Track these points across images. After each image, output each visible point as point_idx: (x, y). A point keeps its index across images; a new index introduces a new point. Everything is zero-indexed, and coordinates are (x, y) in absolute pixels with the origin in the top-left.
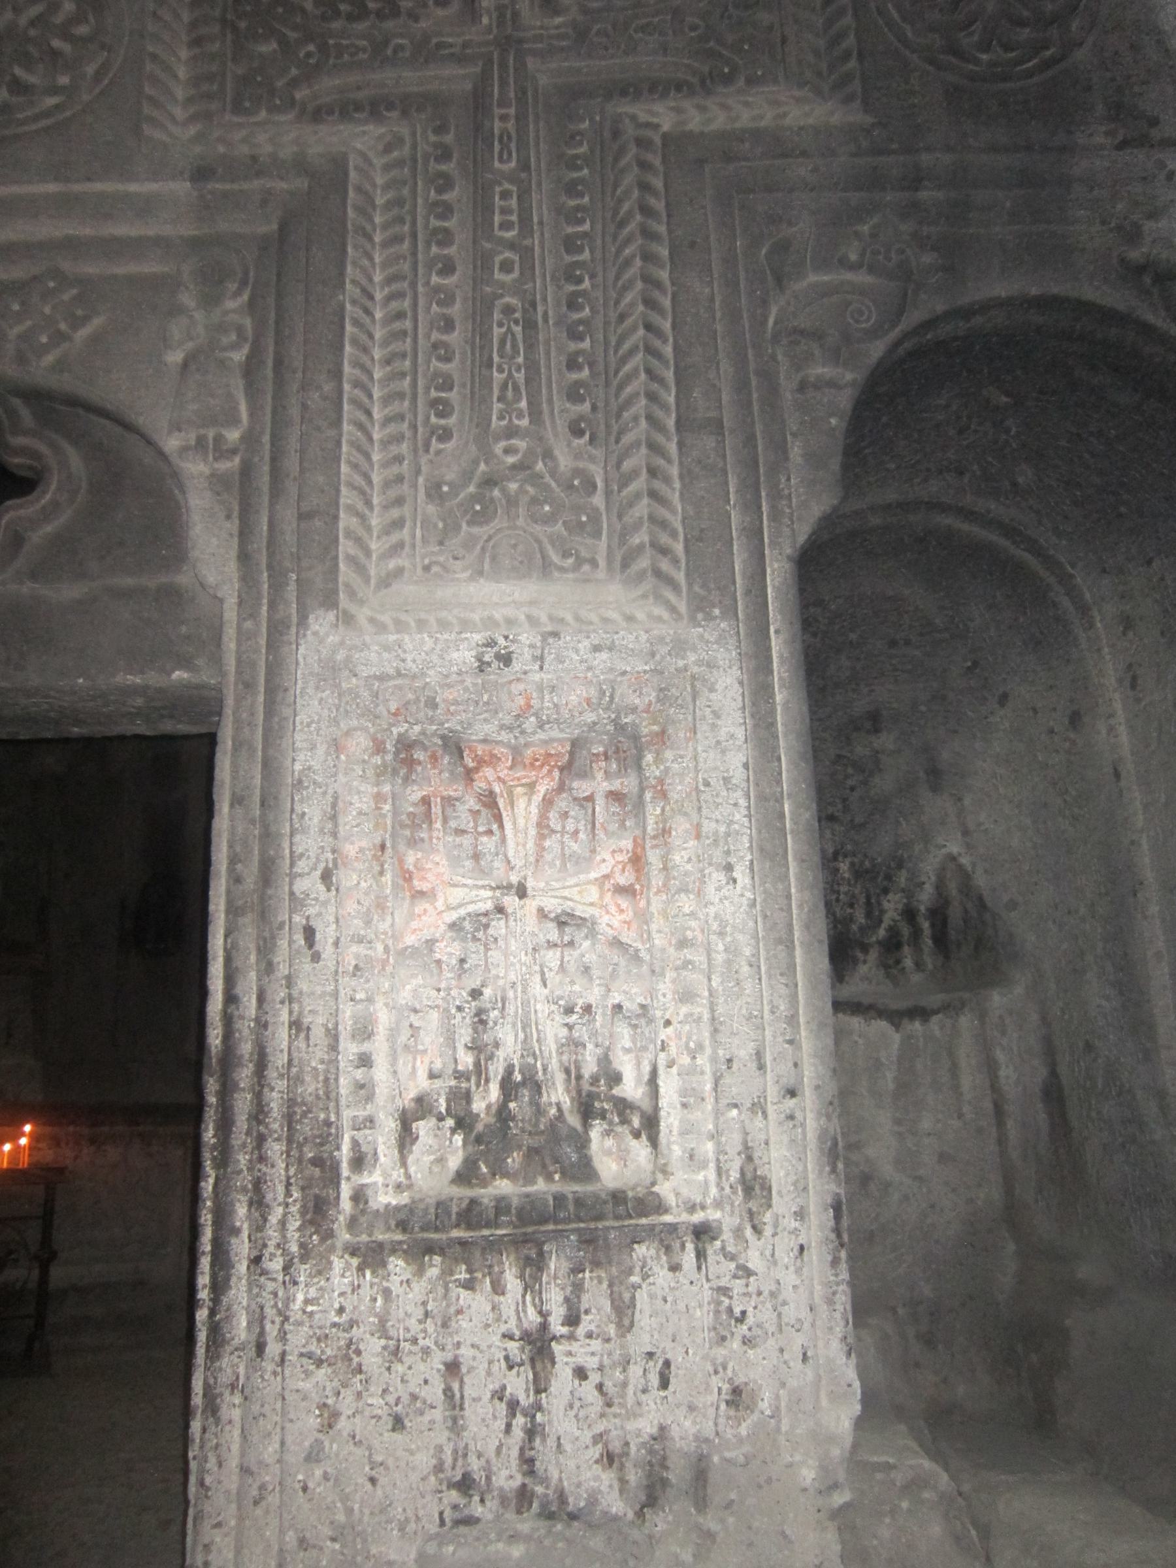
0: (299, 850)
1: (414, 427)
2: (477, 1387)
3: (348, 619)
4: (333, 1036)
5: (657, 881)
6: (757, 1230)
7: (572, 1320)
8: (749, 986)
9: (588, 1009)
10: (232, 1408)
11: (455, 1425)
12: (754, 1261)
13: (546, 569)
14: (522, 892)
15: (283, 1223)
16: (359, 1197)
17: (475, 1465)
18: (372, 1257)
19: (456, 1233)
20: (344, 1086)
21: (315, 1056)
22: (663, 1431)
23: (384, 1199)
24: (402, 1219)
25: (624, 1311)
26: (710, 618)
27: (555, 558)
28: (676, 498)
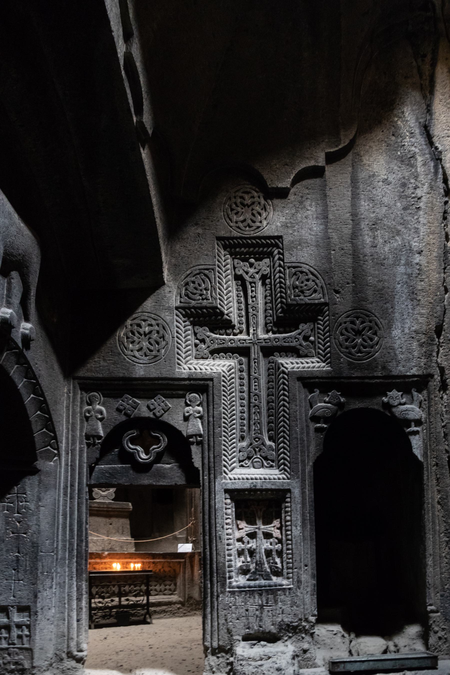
0: (217, 522)
1: (237, 435)
3: (225, 478)
5: (284, 528)
7: (267, 603)
10: (209, 617)
12: (299, 594)
13: (263, 466)
15: (217, 586)
16: (230, 583)
17: (251, 626)
18: (233, 593)
19: (247, 589)
21: (222, 560)
22: (282, 620)
23: (234, 584)
25: (276, 602)
26: (294, 479)
27: (266, 464)
28: (288, 454)
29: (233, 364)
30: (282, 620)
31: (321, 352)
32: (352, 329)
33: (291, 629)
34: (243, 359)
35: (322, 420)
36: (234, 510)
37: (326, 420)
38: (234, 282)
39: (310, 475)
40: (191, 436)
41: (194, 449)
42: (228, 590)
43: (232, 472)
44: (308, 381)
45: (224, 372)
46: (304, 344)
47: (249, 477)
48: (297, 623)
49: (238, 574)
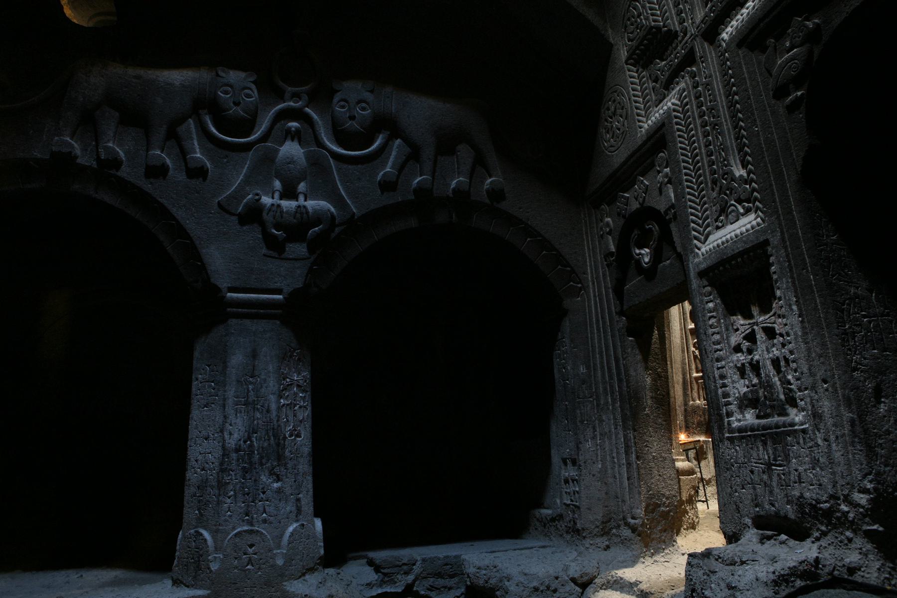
4: (714, 377)
6: (819, 430)
7: (775, 460)
11: (754, 489)
12: (820, 442)
14: (757, 324)
16: (729, 423)
22: (802, 496)
23: (735, 425)
24: (740, 430)
25: (787, 458)
29: (682, 85)
30: (802, 496)
33: (822, 516)
35: (791, 86)
37: (797, 81)
40: (666, 212)
41: (673, 228)
43: (707, 242)
44: (753, 38)
45: (673, 104)
49: (742, 408)
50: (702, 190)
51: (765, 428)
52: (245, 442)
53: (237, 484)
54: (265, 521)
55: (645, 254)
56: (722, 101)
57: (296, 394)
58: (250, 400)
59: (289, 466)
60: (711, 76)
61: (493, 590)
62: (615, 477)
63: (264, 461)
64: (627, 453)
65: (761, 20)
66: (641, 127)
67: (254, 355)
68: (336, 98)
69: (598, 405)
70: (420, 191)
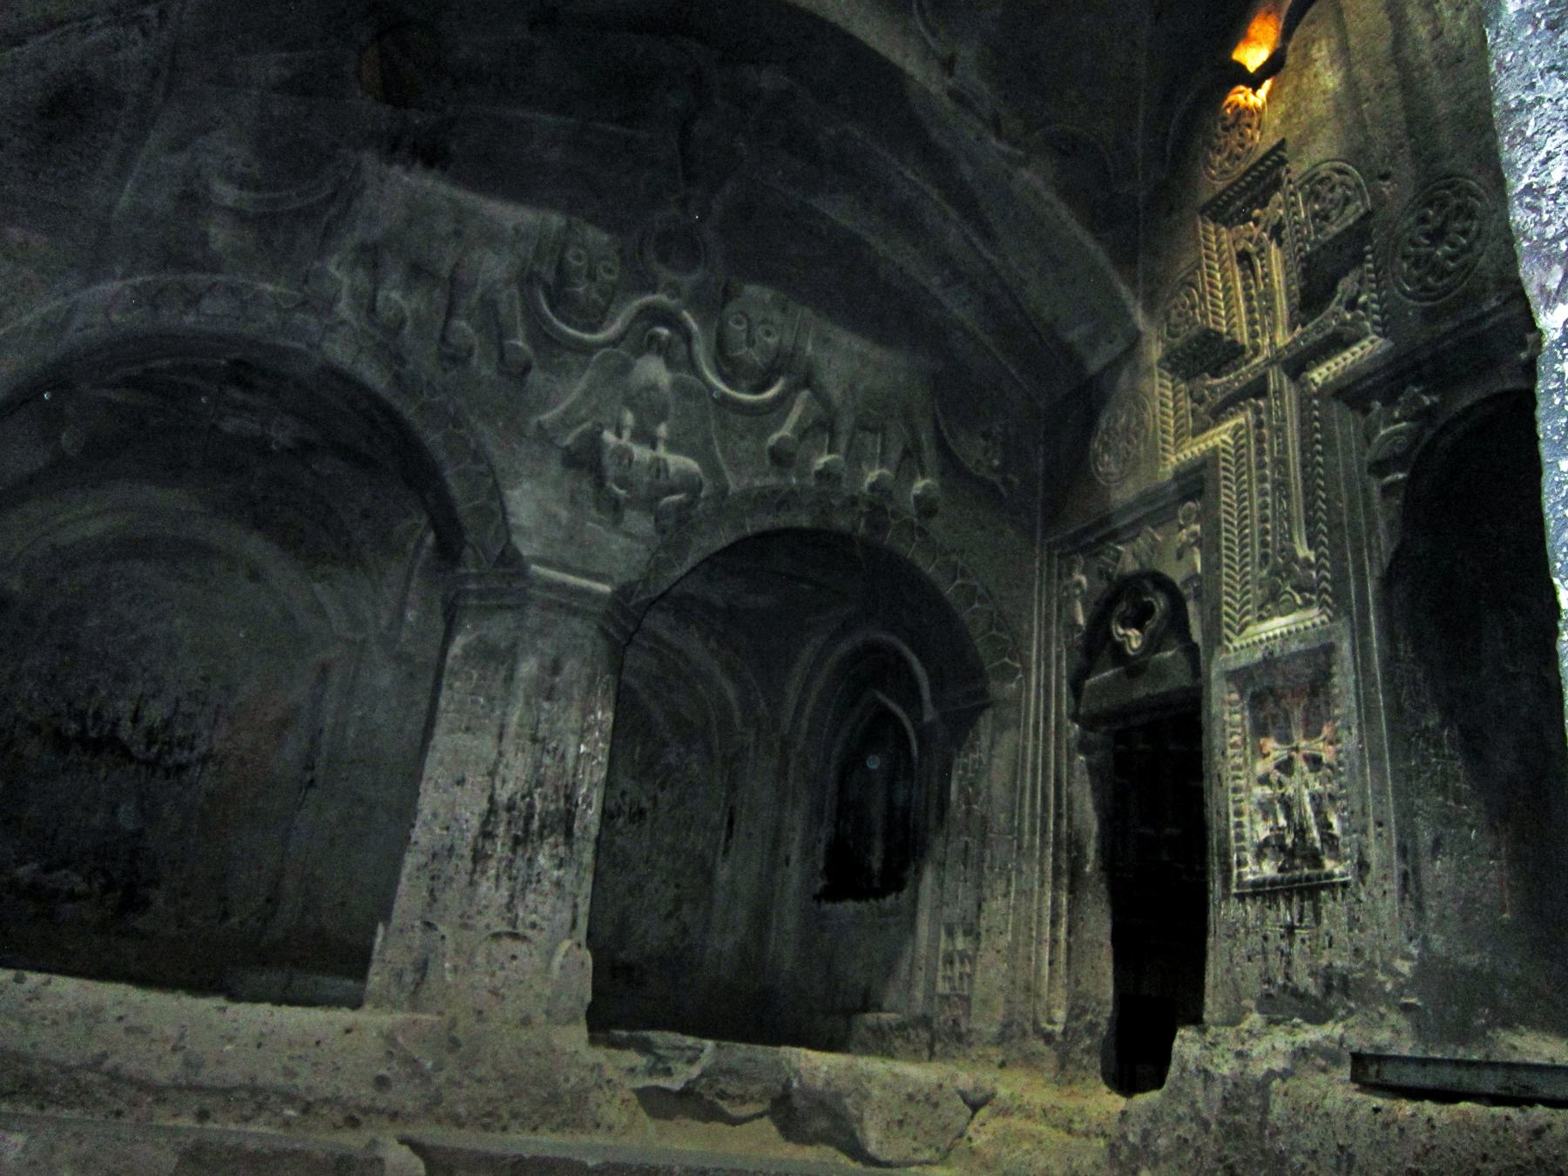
2: (1270, 946)
3: (1227, 650)
7: (1301, 920)
8: (1359, 779)
9: (1320, 797)
12: (1363, 896)
13: (1293, 608)
14: (1297, 749)
16: (1240, 875)
17: (1271, 974)
18: (1241, 897)
20: (1232, 833)
22: (1330, 965)
23: (1250, 877)
24: (1255, 884)
25: (1317, 918)
27: (1299, 601)
29: (1241, 420)
30: (1330, 965)
31: (1376, 317)
32: (1428, 236)
34: (1261, 403)
36: (1247, 713)
38: (1237, 269)
39: (1376, 601)
41: (1191, 607)
42: (1234, 890)
45: (1224, 442)
46: (1349, 316)
47: (1264, 636)
48: (1361, 975)
50: (1246, 565)
51: (1293, 881)
52: (523, 797)
53: (500, 860)
54: (533, 926)
55: (1134, 639)
56: (1294, 456)
57: (596, 742)
58: (540, 735)
59: (575, 847)
60: (1284, 420)
61: (838, 1096)
62: (1029, 959)
63: (546, 833)
64: (1054, 923)
65: (1369, 375)
66: (1165, 459)
67: (556, 668)
68: (732, 307)
69: (1020, 847)
70: (825, 475)
